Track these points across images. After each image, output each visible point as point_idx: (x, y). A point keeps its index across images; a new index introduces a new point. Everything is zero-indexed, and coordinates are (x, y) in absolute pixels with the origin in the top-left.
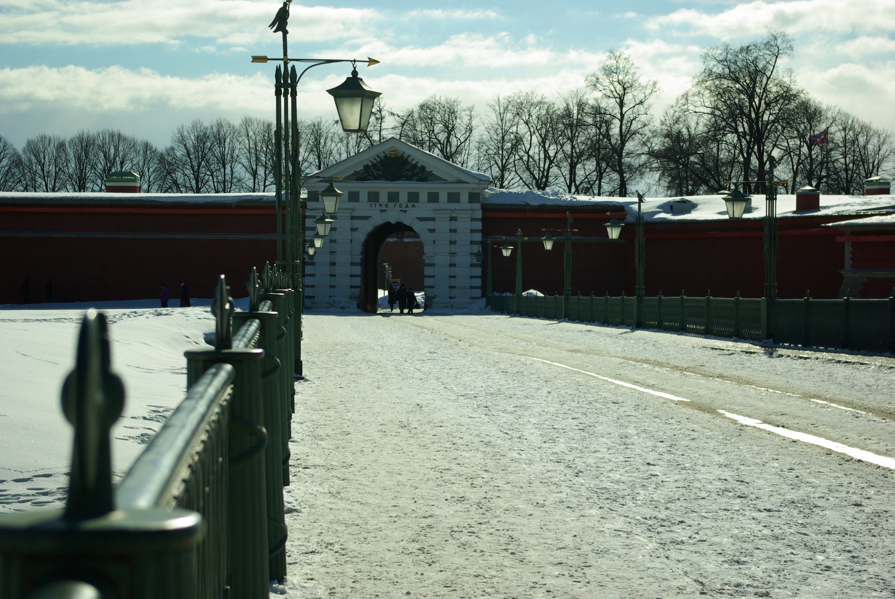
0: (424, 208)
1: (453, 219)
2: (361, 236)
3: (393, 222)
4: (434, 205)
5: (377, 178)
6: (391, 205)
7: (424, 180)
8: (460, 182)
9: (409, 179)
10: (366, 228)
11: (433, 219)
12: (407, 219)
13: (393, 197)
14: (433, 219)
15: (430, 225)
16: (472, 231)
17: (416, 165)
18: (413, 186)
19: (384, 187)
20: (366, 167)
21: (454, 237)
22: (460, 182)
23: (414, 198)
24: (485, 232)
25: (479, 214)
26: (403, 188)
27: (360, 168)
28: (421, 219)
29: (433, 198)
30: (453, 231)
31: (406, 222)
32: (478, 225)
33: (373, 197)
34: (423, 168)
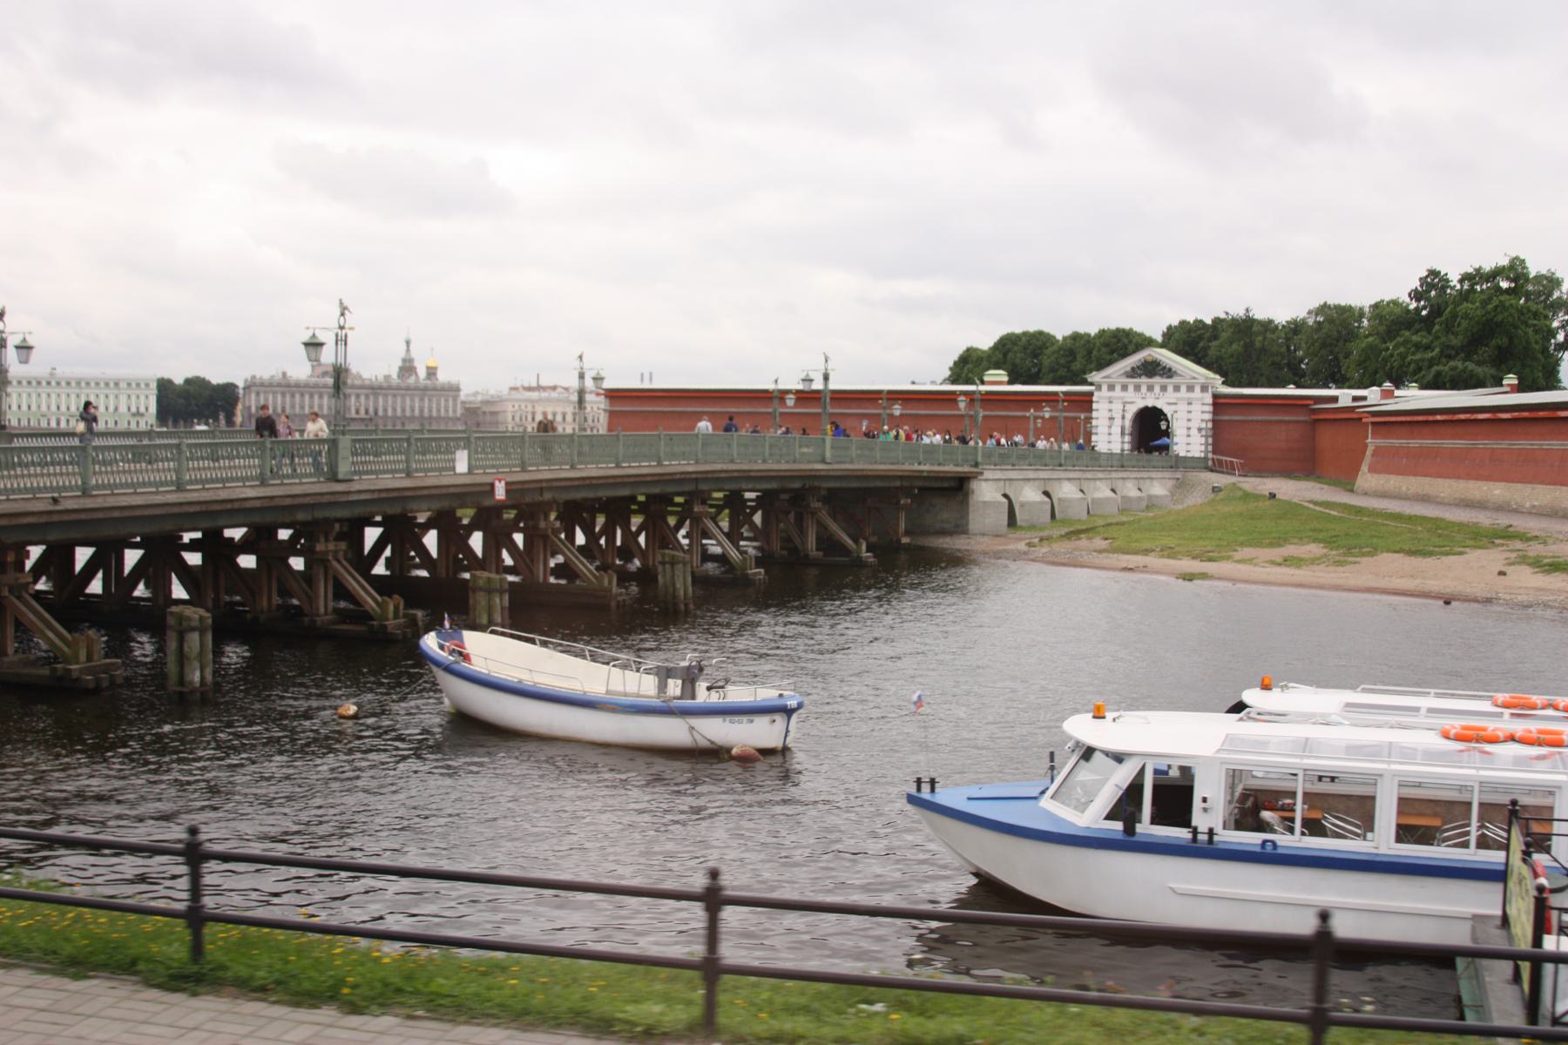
0: (1170, 395)
1: (1190, 404)
2: (1130, 416)
3: (1150, 405)
4: (1178, 395)
5: (1140, 376)
6: (1149, 394)
7: (1170, 377)
8: (1194, 378)
9: (1161, 376)
10: (1132, 411)
11: (1175, 404)
12: (1159, 404)
13: (1150, 388)
14: (1175, 404)
15: (1173, 408)
16: (1203, 412)
17: (1164, 368)
18: (1165, 381)
19: (1144, 380)
20: (1133, 369)
21: (1190, 416)
22: (1194, 378)
23: (1164, 388)
24: (1215, 413)
25: (1209, 400)
26: (1157, 380)
27: (1129, 369)
28: (1169, 404)
29: (1177, 388)
30: (1190, 412)
31: (1159, 406)
32: (1210, 408)
33: (1137, 388)
34: (1170, 369)
